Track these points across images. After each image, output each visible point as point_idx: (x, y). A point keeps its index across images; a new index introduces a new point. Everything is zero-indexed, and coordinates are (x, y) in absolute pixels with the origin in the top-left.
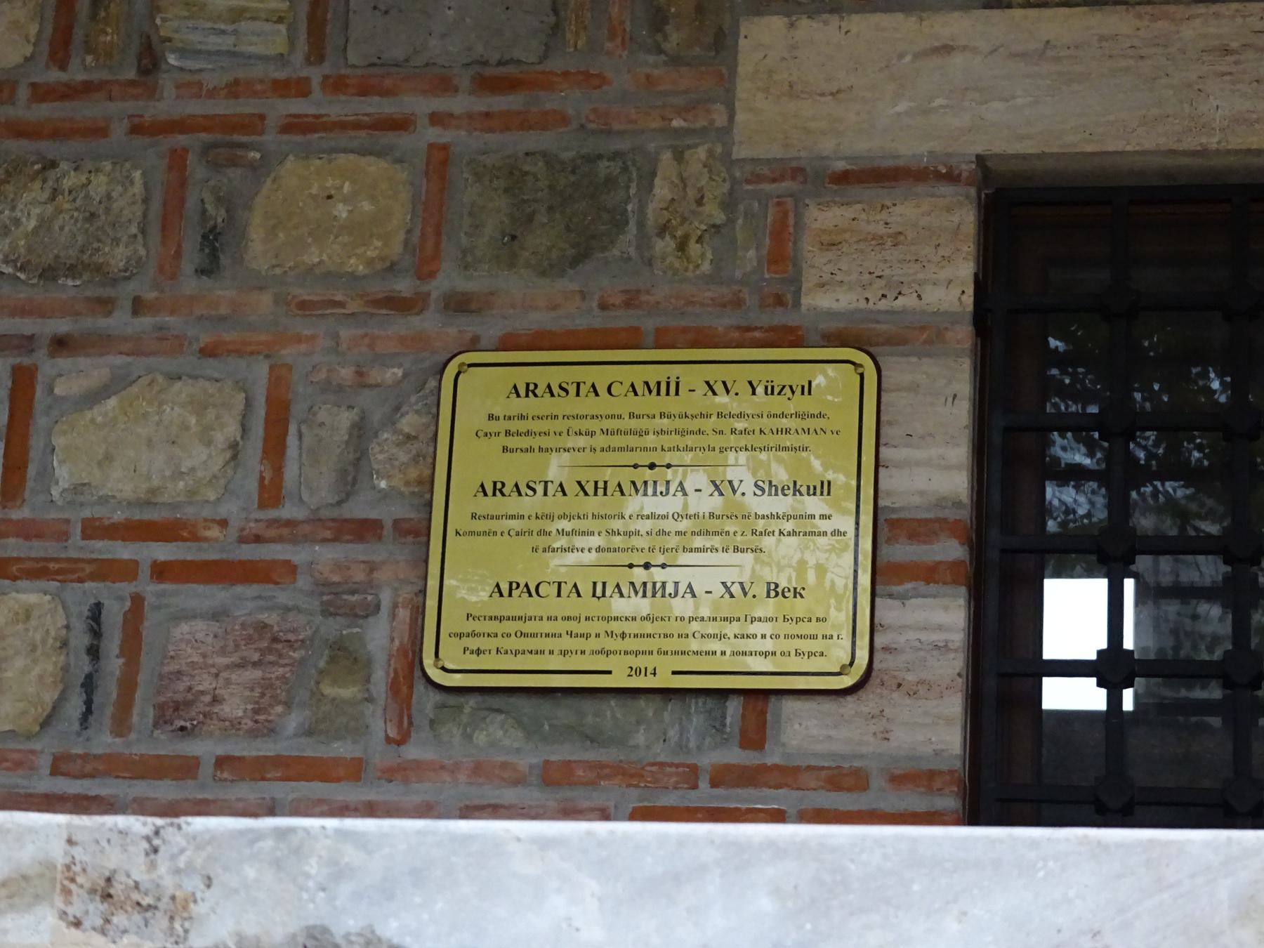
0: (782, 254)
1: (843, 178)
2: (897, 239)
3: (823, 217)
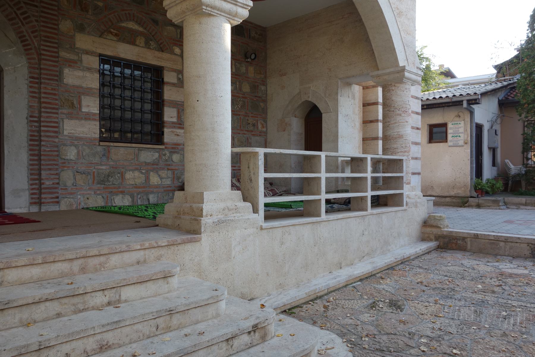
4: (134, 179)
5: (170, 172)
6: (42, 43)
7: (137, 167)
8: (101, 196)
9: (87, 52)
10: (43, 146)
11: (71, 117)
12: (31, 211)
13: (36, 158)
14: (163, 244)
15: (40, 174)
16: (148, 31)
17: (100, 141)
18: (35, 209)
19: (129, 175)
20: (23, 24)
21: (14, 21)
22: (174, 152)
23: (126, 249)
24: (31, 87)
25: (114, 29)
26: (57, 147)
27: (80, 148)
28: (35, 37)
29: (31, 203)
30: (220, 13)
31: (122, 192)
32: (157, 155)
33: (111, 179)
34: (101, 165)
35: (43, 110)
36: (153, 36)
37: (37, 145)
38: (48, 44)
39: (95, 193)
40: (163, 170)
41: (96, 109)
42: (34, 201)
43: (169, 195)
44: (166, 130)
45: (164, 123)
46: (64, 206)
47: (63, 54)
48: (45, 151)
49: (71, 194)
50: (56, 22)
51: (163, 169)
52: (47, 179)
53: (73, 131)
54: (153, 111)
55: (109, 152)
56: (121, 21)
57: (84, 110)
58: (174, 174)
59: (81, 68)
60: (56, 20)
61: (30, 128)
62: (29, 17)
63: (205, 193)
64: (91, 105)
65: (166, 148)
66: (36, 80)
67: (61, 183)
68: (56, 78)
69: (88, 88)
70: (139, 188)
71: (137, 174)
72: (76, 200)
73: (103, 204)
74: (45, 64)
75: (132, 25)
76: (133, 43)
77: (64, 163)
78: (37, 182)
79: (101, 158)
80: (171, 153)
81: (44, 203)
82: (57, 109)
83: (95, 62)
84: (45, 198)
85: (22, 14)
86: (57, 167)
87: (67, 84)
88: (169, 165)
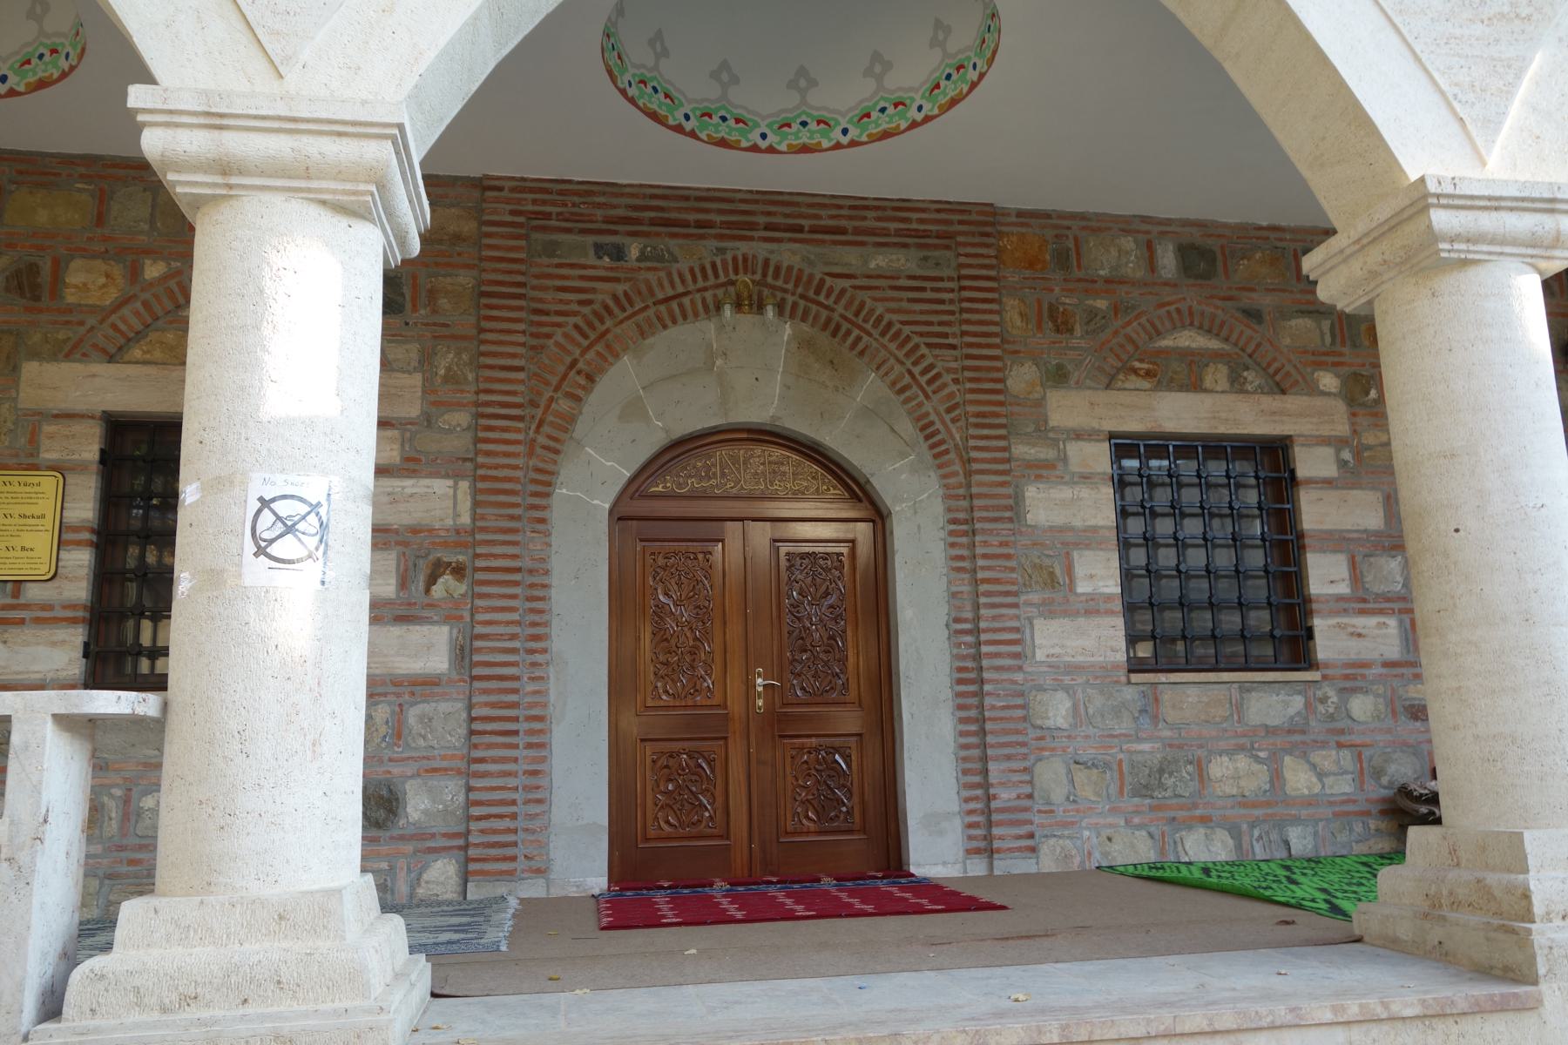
0: (34, 440)
1: (56, 416)
2: (73, 436)
3: (48, 428)
4: (1236, 777)
5: (1346, 755)
6: (972, 431)
7: (1242, 741)
8: (1144, 833)
9: (1079, 435)
10: (989, 694)
11: (1050, 610)
12: (970, 874)
13: (973, 728)
14: (1408, 1012)
15: (985, 772)
16: (1236, 344)
17: (1130, 671)
18: (977, 868)
19: (1219, 768)
20: (927, 397)
21: (908, 394)
22: (1354, 690)
23: (1289, 1018)
24: (952, 545)
25: (1141, 361)
26: (1021, 694)
27: (1080, 695)
28: (954, 421)
29: (969, 852)
30: (1498, 249)
31: (1205, 820)
32: (1298, 702)
33: (1170, 782)
34: (1139, 740)
35: (983, 600)
36: (1250, 356)
37: (974, 694)
38: (986, 432)
40: (1323, 748)
41: (1111, 582)
42: (975, 844)
43: (1351, 830)
44: (1319, 624)
45: (1310, 601)
46: (1047, 862)
47: (1021, 450)
48: (993, 707)
49: (1065, 825)
50: (1000, 375)
51: (1324, 745)
52: (1001, 784)
53: (1057, 650)
54: (1272, 568)
55: (1156, 700)
56: (1159, 333)
57: (1083, 587)
59: (1067, 478)
60: (998, 370)
61: (955, 651)
62: (938, 376)
63: (1527, 835)
64: (1099, 575)
65: (1325, 677)
66: (963, 526)
67: (1036, 794)
68: (1007, 514)
69: (1087, 529)
70: (1254, 805)
71: (1242, 762)
72: (1079, 843)
73: (1152, 856)
74: (980, 484)
75: (1189, 339)
77: (1042, 738)
78: (979, 792)
79: (1136, 719)
80: (1346, 692)
81: (999, 851)
82: (1015, 594)
83: (1098, 457)
84: (1001, 838)
85: (923, 373)
86: (1024, 750)
88: (1342, 732)
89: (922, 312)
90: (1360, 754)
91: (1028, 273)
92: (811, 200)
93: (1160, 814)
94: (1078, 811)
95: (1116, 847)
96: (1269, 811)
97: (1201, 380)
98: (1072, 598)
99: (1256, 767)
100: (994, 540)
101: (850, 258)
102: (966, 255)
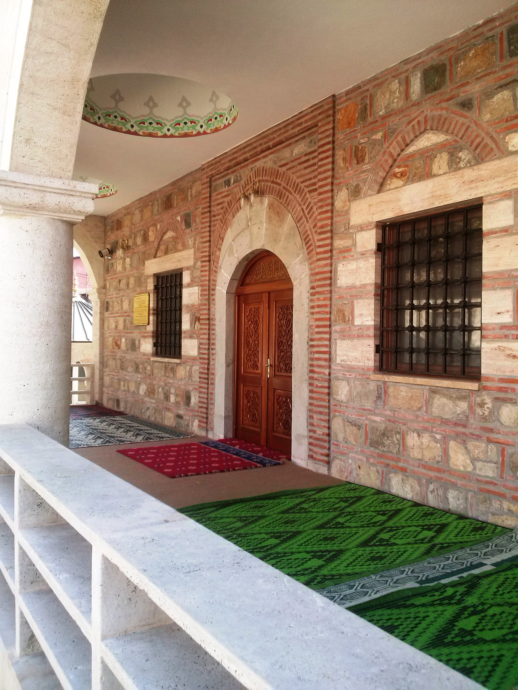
5: (491, 446)
7: (427, 425)
9: (362, 228)
19: (412, 440)
22: (505, 401)
31: (403, 470)
34: (376, 415)
39: (368, 460)
41: (370, 318)
47: (339, 243)
51: (478, 437)
57: (356, 323)
58: (503, 455)
76: (428, 175)
87: (340, 287)
88: (491, 430)
89: (308, 174)
90: (503, 450)
91: (348, 130)
92: (283, 125)
93: (383, 460)
94: (347, 448)
95: (362, 472)
96: (439, 475)
97: (431, 169)
98: (352, 328)
99: (433, 444)
100: (321, 297)
101: (286, 154)
102: (327, 130)
